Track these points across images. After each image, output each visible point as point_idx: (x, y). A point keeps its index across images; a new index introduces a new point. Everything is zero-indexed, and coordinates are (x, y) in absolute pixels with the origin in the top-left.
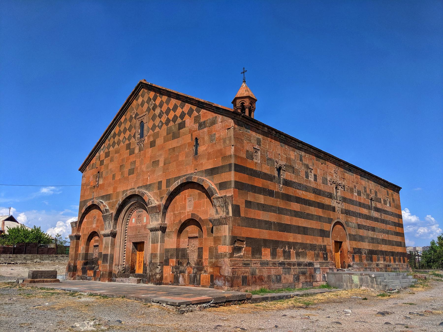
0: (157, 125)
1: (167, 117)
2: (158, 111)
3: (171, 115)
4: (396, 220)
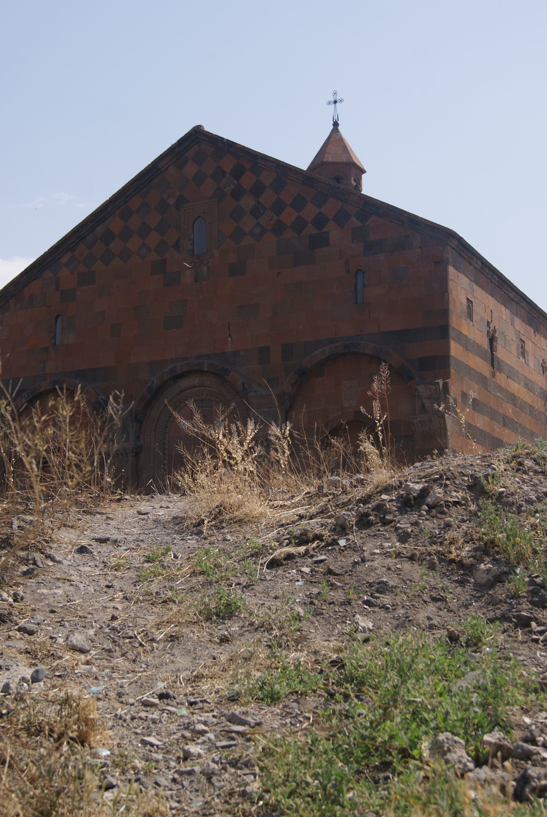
1: (275, 217)
2: (247, 202)
3: (289, 216)
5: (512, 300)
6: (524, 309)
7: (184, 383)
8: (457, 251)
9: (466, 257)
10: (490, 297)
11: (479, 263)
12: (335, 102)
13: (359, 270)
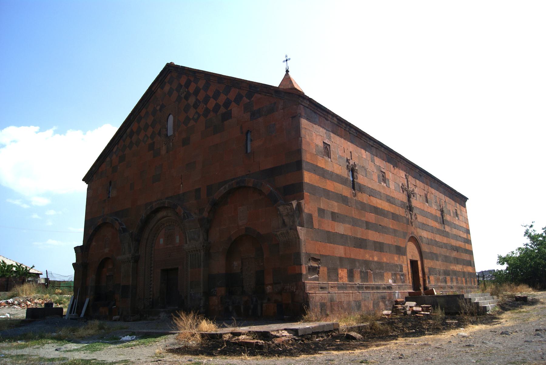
0: (191, 117)
1: (205, 106)
2: (192, 100)
3: (212, 104)
4: (465, 236)
5: (372, 146)
6: (383, 152)
7: (159, 215)
8: (311, 109)
9: (321, 114)
10: (349, 143)
11: (335, 119)
12: (287, 60)
13: (248, 131)
